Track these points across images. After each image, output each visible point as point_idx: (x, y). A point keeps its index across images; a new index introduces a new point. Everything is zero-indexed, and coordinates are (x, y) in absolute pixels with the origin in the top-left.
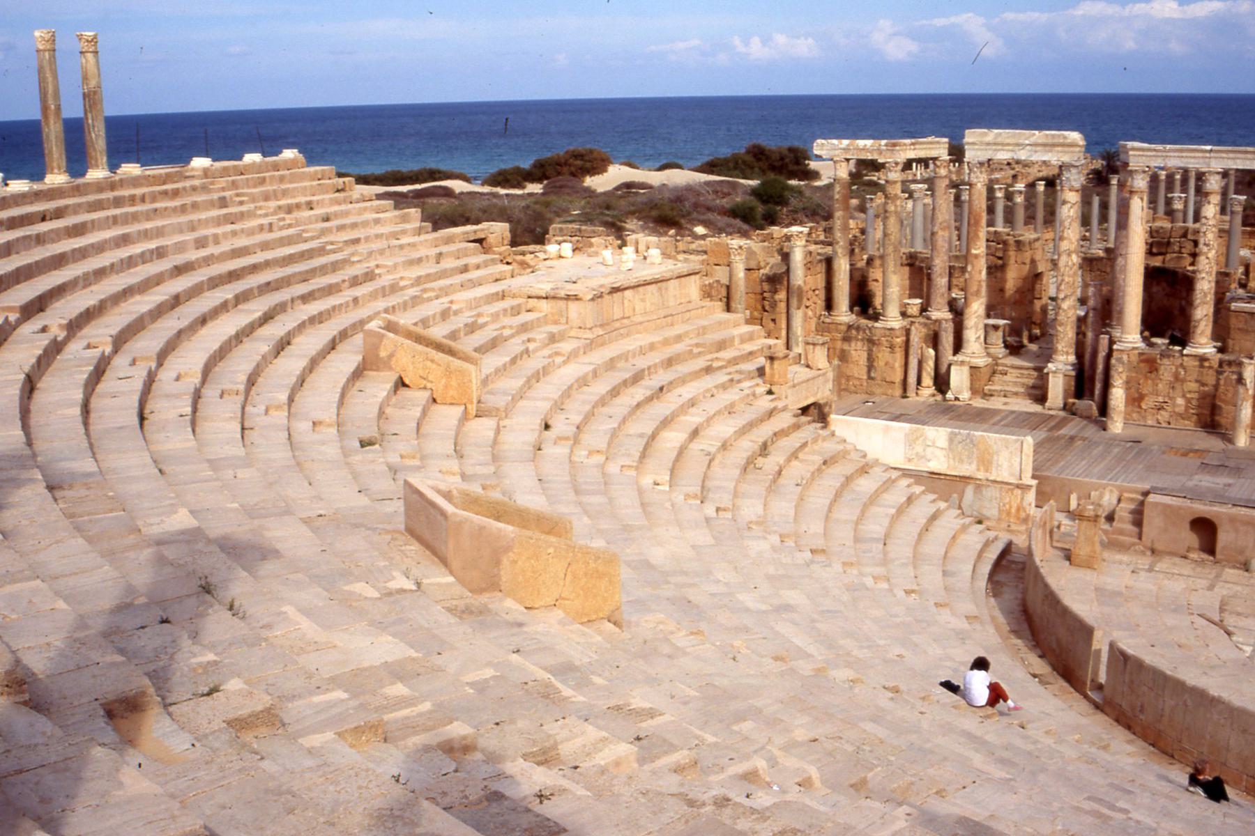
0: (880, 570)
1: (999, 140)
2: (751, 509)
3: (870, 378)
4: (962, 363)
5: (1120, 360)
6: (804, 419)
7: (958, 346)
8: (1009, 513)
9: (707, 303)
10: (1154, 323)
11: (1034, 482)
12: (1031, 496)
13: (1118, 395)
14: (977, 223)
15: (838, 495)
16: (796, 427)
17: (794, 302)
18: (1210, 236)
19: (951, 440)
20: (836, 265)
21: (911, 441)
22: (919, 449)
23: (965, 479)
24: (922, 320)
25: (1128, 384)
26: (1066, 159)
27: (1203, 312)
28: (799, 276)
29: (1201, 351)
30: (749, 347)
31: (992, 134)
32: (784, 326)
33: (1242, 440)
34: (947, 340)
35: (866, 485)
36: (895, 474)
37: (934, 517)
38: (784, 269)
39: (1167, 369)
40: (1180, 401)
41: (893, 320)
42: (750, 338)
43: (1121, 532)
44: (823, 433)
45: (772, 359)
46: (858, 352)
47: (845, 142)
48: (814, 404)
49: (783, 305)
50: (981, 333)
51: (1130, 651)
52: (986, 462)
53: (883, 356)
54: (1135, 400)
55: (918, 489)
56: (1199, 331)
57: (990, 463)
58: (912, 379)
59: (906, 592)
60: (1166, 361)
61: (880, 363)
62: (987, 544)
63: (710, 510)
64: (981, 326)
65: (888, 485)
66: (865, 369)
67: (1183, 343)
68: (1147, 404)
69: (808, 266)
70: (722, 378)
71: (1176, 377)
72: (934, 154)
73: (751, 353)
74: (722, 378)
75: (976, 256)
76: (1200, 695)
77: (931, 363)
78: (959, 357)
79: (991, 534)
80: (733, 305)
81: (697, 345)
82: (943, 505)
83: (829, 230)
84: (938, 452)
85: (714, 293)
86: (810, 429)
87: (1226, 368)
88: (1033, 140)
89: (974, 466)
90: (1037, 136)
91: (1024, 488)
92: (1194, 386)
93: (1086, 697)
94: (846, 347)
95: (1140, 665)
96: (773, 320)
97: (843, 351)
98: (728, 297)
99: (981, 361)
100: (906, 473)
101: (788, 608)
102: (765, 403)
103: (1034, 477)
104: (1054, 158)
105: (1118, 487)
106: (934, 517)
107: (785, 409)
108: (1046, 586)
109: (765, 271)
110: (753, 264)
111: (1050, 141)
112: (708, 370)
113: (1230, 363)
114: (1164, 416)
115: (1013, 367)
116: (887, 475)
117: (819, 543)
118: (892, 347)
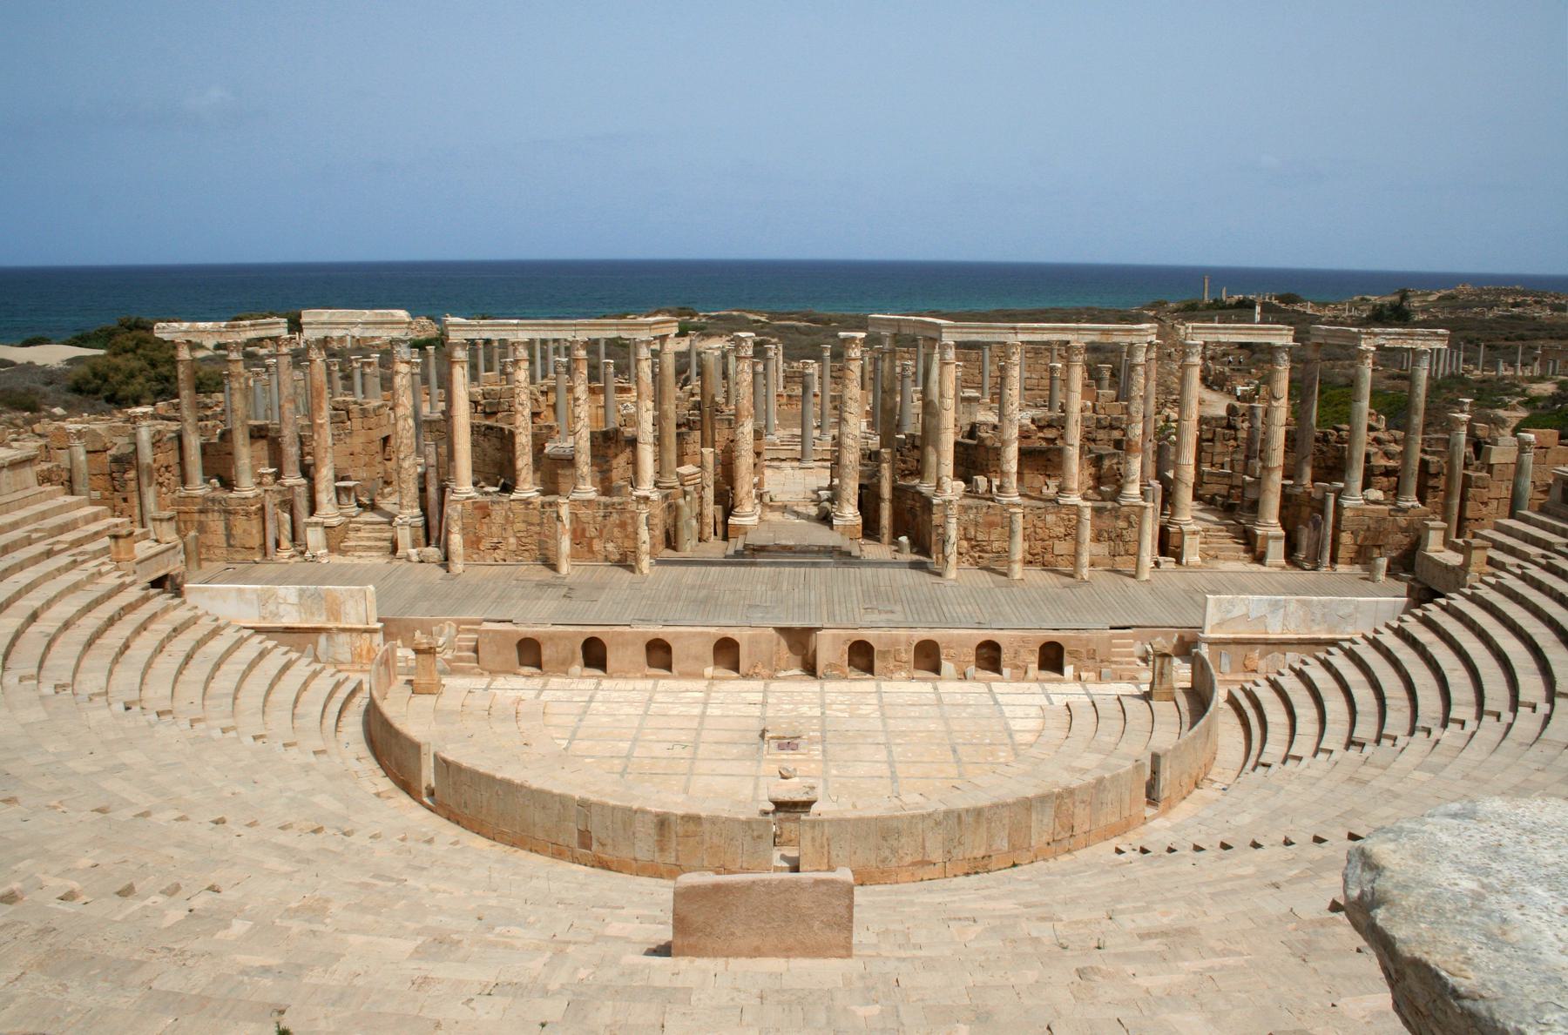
0: (229, 722)
1: (334, 319)
2: (92, 681)
3: (230, 545)
4: (316, 524)
5: (454, 510)
6: (153, 591)
7: (313, 510)
8: (360, 656)
9: (48, 488)
10: (482, 475)
11: (379, 625)
12: (379, 638)
13: (456, 540)
14: (320, 395)
15: (189, 658)
16: (145, 599)
17: (145, 480)
18: (523, 397)
19: (301, 594)
20: (186, 441)
21: (263, 600)
22: (272, 607)
23: (317, 630)
24: (275, 487)
25: (464, 529)
26: (396, 334)
27: (524, 461)
28: (146, 455)
29: (525, 495)
30: (94, 527)
31: (326, 315)
32: (136, 501)
33: (565, 567)
34: (302, 504)
35: (217, 646)
36: (246, 633)
37: (286, 667)
38: (131, 448)
39: (498, 514)
40: (512, 540)
41: (247, 488)
42: (95, 518)
43: (461, 659)
44: (177, 601)
45: (116, 537)
46: (216, 523)
47: (186, 325)
48: (165, 577)
49: (133, 484)
50: (333, 495)
51: (450, 758)
52: (335, 613)
53: (240, 524)
54: (473, 543)
55: (270, 644)
56: (521, 478)
57: (339, 613)
58: (271, 543)
59: (255, 738)
60: (496, 507)
61: (237, 531)
62: (338, 685)
63: (47, 689)
64: (332, 488)
65: (239, 643)
66: (223, 538)
67: (508, 488)
68: (485, 544)
69: (156, 444)
70: (64, 559)
71: (507, 517)
72: (274, 332)
73: (96, 533)
74: (64, 559)
75: (321, 425)
76: (508, 786)
77: (288, 527)
78: (314, 519)
79: (341, 676)
80: (76, 487)
81: (36, 530)
82: (294, 655)
83: (177, 408)
84: (289, 608)
85: (54, 477)
86: (160, 600)
87: (548, 509)
88: (363, 319)
89: (324, 618)
90: (368, 315)
91: (373, 631)
92: (522, 526)
93: (422, 803)
94: (203, 517)
95: (459, 769)
96: (125, 500)
97: (200, 523)
98: (70, 481)
99: (334, 522)
100: (258, 630)
101: (124, 766)
102: (111, 580)
103: (379, 620)
104: (385, 334)
105: (455, 621)
106: (286, 667)
107: (133, 583)
108: (381, 714)
109: (113, 452)
110: (99, 447)
111: (379, 319)
112: (49, 554)
113: (550, 504)
114: (499, 554)
115: (367, 523)
116: (238, 635)
117: (166, 705)
118: (247, 514)
